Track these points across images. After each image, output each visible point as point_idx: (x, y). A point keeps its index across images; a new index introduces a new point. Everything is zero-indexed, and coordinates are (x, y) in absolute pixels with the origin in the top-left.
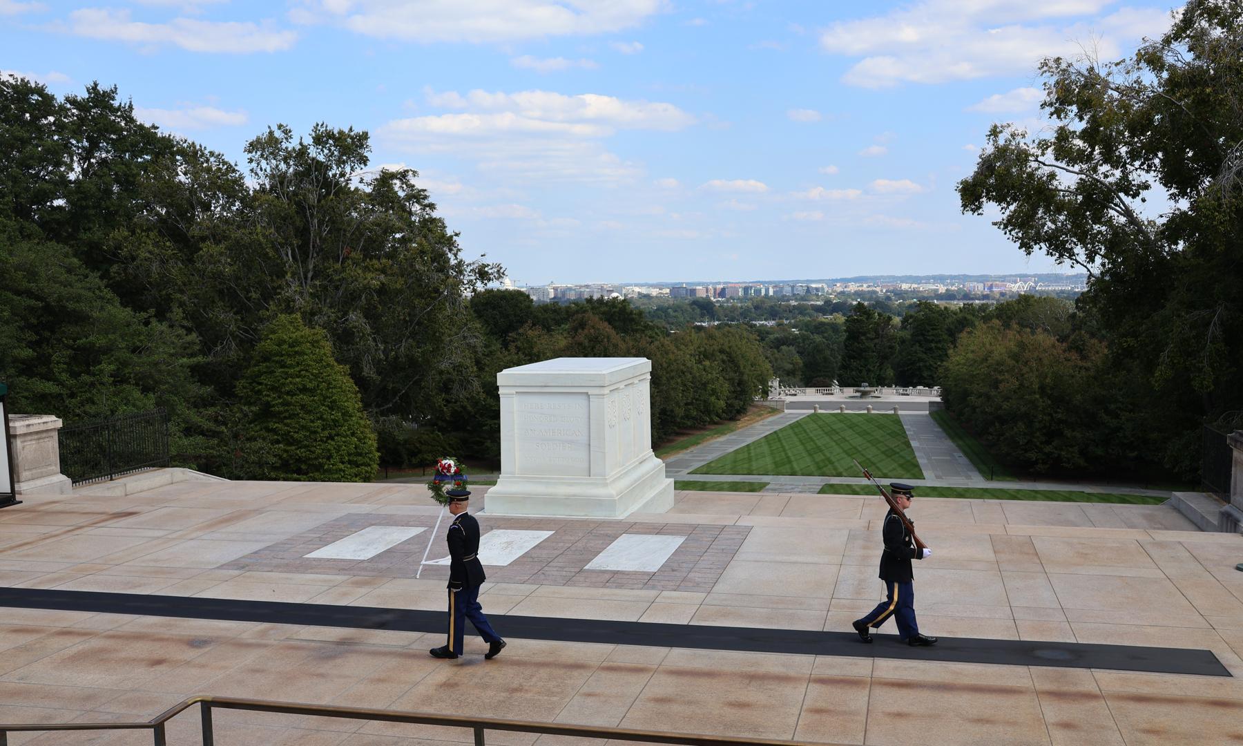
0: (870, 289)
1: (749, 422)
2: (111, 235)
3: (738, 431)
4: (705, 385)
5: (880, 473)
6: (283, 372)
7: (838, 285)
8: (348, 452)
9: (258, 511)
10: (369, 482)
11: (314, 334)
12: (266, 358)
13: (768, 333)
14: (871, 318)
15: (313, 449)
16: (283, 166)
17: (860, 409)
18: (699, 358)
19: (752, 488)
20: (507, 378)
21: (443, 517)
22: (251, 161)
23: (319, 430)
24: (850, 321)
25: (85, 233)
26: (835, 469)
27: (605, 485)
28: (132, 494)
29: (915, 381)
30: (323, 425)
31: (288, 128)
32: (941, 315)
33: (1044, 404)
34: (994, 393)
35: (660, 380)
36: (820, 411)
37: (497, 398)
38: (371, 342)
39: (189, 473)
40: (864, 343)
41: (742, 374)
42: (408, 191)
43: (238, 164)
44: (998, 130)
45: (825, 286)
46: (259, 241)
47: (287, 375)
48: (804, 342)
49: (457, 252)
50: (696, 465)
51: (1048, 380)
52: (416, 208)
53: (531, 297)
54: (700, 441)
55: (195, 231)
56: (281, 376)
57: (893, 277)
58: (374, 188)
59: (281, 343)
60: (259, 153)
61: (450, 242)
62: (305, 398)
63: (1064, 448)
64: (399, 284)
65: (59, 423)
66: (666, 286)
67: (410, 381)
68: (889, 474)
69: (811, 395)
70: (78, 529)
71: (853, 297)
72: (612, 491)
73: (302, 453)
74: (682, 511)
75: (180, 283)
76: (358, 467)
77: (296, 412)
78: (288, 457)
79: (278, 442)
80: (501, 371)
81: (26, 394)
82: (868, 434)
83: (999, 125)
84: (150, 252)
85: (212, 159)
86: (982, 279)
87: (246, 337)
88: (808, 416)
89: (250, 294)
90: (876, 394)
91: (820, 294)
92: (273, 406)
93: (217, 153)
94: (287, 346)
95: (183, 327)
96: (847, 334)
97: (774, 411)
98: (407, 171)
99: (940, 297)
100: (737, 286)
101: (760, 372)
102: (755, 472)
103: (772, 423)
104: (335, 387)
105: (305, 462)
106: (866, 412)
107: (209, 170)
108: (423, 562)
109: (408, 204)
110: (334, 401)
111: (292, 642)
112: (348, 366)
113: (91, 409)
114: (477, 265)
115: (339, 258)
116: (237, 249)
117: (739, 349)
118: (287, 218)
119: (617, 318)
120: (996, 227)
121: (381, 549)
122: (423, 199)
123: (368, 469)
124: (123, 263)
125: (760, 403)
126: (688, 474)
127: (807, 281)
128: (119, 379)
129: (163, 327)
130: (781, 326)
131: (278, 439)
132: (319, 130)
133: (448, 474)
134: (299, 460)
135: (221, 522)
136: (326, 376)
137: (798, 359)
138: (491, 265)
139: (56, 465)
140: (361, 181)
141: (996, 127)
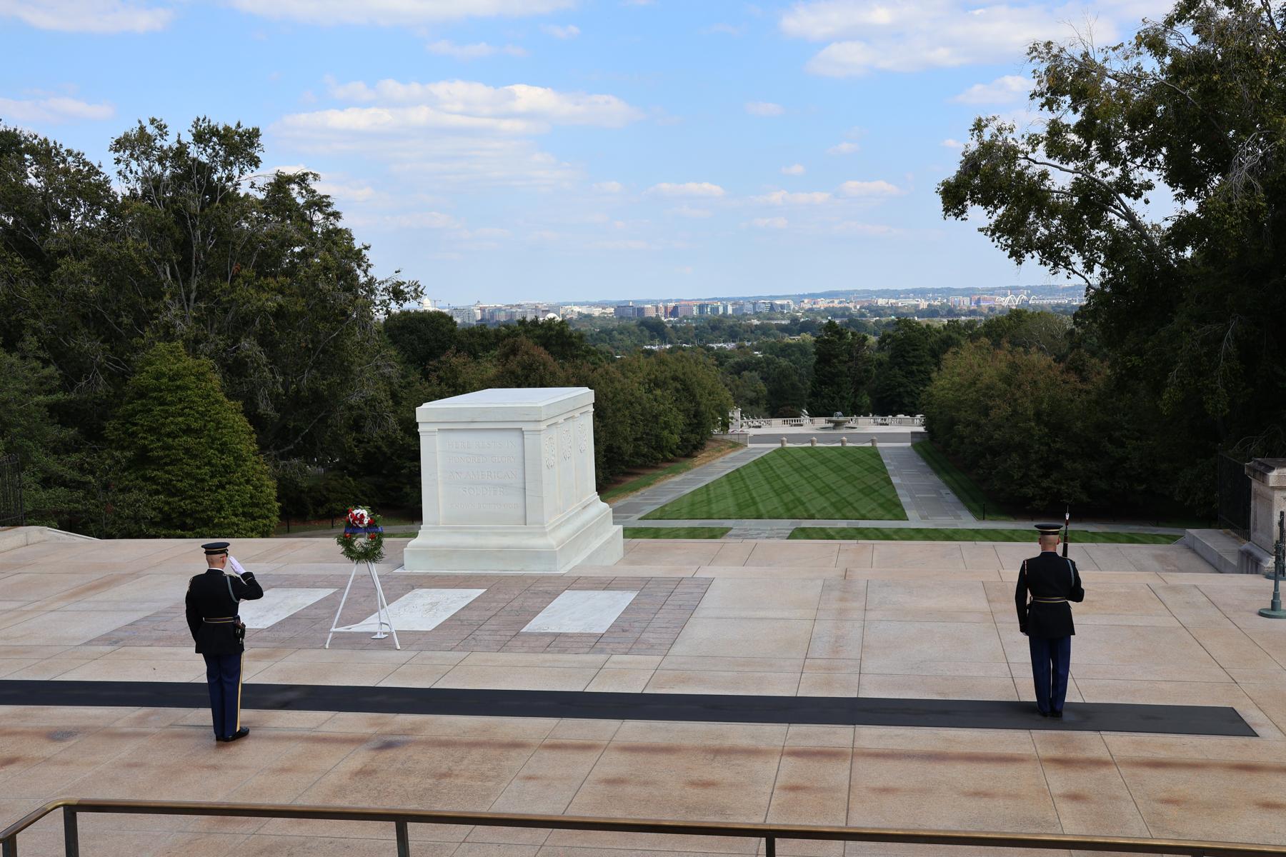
0: (842, 305)
1: (708, 459)
3: (695, 469)
4: (656, 417)
5: (857, 514)
6: (162, 410)
7: (806, 301)
8: (242, 503)
9: (135, 575)
12: (142, 394)
13: (727, 357)
14: (843, 339)
15: (199, 500)
16: (157, 168)
17: (833, 442)
18: (649, 387)
19: (713, 534)
20: (427, 413)
21: (355, 576)
22: (118, 161)
24: (820, 342)
26: (807, 510)
27: (544, 534)
29: (895, 409)
30: (212, 472)
31: (162, 123)
32: (923, 334)
33: (1040, 433)
34: (984, 421)
35: (604, 413)
36: (788, 445)
37: (417, 436)
40: (836, 367)
41: (698, 404)
42: (308, 197)
43: (102, 165)
44: (983, 124)
45: (791, 303)
46: (130, 256)
47: (168, 414)
48: (768, 367)
49: (367, 268)
50: (649, 509)
51: (1044, 406)
52: (318, 217)
53: (455, 319)
54: (652, 482)
55: (51, 245)
56: (160, 415)
57: (868, 291)
58: (268, 194)
59: (159, 375)
60: (128, 152)
61: (358, 256)
62: (189, 440)
63: (1064, 481)
66: (610, 304)
67: (314, 419)
68: (868, 515)
69: (777, 427)
71: (823, 314)
72: (552, 541)
73: (186, 504)
74: (633, 563)
75: (33, 306)
79: (157, 492)
80: (421, 405)
82: (843, 469)
83: (984, 118)
85: (70, 159)
86: (968, 292)
88: (774, 451)
89: (120, 319)
90: (852, 424)
91: (785, 311)
92: (151, 450)
93: (75, 152)
94: (167, 380)
95: (38, 358)
96: (817, 356)
97: (735, 445)
98: (307, 174)
99: (921, 313)
100: (690, 303)
101: (718, 402)
102: (715, 516)
103: (733, 459)
104: (225, 427)
105: (190, 515)
106: (840, 445)
107: (66, 172)
108: (333, 629)
109: (308, 213)
110: (224, 444)
111: (176, 730)
112: (240, 402)
114: (390, 283)
116: (104, 266)
117: (695, 375)
118: (164, 230)
119: (554, 342)
120: (983, 233)
121: (284, 615)
122: (325, 206)
125: (719, 437)
126: (639, 519)
127: (771, 297)
130: (742, 349)
132: (201, 126)
133: (361, 526)
134: (184, 513)
136: (214, 414)
137: (762, 386)
138: (407, 283)
140: (253, 186)
141: (980, 120)
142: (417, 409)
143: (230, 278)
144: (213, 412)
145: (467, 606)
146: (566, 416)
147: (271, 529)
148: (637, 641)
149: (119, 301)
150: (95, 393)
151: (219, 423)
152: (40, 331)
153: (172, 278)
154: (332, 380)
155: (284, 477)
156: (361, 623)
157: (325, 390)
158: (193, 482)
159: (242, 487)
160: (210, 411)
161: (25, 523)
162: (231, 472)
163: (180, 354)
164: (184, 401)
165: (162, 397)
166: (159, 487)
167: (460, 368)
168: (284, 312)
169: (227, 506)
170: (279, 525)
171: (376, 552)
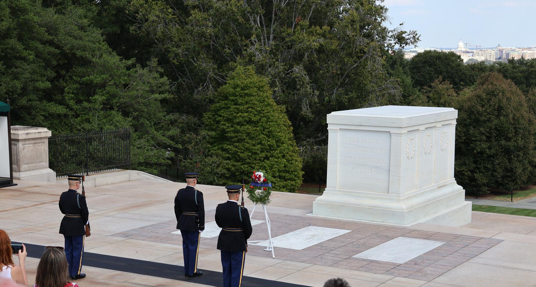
2: (132, 3)
6: (235, 108)
8: (279, 170)
11: (260, 81)
15: (253, 165)
21: (254, 212)
23: (258, 152)
28: (99, 186)
39: (143, 175)
47: (239, 111)
49: (381, 21)
53: (462, 57)
56: (234, 111)
59: (236, 86)
62: (249, 128)
64: (334, 45)
65: (49, 134)
70: (41, 204)
72: (403, 206)
73: (245, 168)
74: (474, 227)
76: (286, 180)
77: (243, 138)
78: (235, 170)
79: (228, 159)
81: (43, 113)
84: (158, 16)
87: (222, 81)
89: (224, 50)
92: (227, 132)
95: (157, 72)
104: (272, 121)
113: (87, 126)
114: (396, 32)
115: (292, 24)
116: (219, 16)
123: (293, 183)
124: (139, 23)
128: (109, 106)
129: (146, 70)
131: (228, 156)
133: (259, 182)
134: (243, 173)
135: (134, 207)
136: (266, 113)
139: (46, 162)
142: (328, 116)
143: (293, 26)
144: (266, 111)
145: (332, 239)
147: (296, 188)
148: (419, 271)
149: (224, 38)
150: (207, 95)
151: (269, 118)
152: (178, 55)
153: (261, 25)
154: (352, 95)
155: (316, 156)
156: (266, 241)
157: (346, 101)
158: (250, 154)
159: (279, 159)
160: (264, 111)
161: (131, 168)
162: (274, 150)
163: (250, 73)
164: (249, 103)
165: (236, 99)
166: (230, 156)
167: (443, 92)
168: (324, 50)
170: (302, 186)
171: (266, 198)
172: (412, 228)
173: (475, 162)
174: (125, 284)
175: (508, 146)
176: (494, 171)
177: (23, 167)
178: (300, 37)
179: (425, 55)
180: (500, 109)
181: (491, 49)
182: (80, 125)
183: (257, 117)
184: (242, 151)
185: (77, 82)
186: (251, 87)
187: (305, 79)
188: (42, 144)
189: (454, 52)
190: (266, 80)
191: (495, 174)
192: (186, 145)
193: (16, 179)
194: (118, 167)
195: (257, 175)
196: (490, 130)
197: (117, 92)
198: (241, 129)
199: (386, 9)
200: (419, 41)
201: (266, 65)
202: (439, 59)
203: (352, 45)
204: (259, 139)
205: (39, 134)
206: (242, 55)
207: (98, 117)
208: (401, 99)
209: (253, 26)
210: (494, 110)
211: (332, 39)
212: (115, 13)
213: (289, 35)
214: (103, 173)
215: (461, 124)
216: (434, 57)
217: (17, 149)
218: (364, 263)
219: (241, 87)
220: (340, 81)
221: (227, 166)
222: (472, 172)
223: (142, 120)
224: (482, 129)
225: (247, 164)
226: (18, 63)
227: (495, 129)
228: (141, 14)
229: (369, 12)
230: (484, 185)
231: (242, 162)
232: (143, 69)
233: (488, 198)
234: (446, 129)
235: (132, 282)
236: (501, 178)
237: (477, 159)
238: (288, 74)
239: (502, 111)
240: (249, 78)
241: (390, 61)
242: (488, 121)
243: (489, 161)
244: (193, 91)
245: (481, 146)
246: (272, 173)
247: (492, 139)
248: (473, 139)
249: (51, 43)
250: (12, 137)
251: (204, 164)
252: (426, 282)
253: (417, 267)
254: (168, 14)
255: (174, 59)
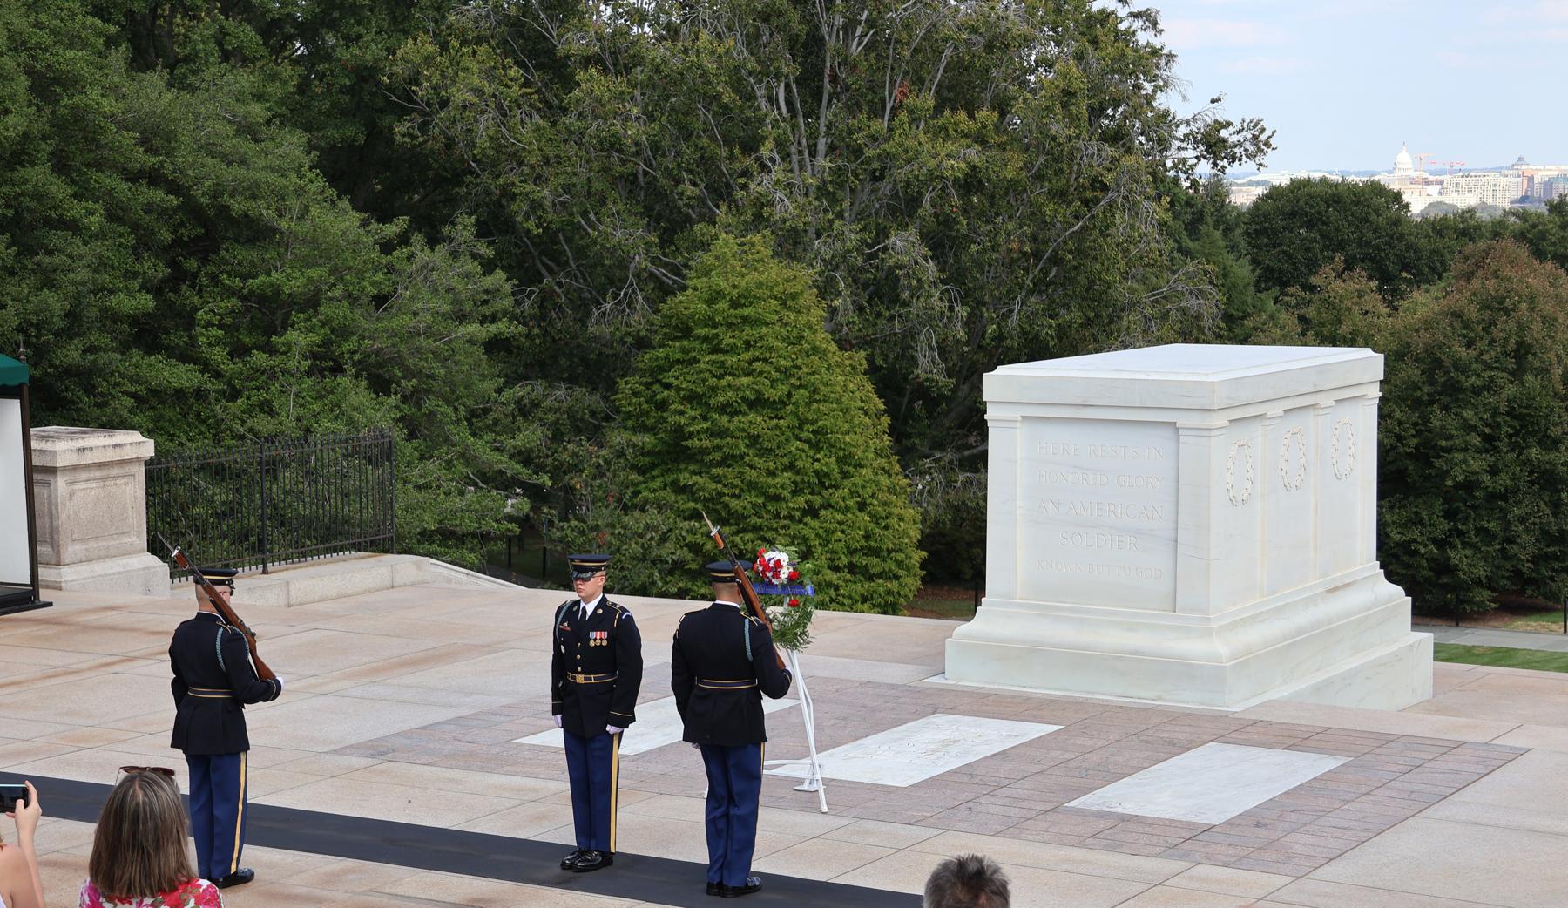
2: (399, 53)
6: (715, 362)
8: (848, 547)
9: (489, 648)
10: (894, 613)
15: (769, 535)
23: (786, 493)
25: (348, 47)
28: (301, 604)
38: (936, 302)
39: (433, 568)
46: (700, 67)
47: (724, 371)
49: (1154, 92)
53: (1406, 198)
56: (711, 372)
59: (714, 297)
62: (756, 421)
64: (1012, 167)
65: (148, 448)
72: (1219, 648)
73: (745, 540)
74: (1441, 710)
76: (870, 578)
77: (737, 452)
79: (696, 515)
84: (478, 91)
87: (675, 281)
89: (680, 188)
92: (691, 435)
95: (474, 256)
113: (264, 424)
114: (1200, 124)
116: (662, 84)
118: (769, 15)
123: (893, 585)
124: (425, 114)
128: (330, 363)
129: (441, 252)
142: (985, 375)
143: (888, 111)
144: (806, 370)
145: (1004, 752)
146: (1289, 404)
149: (678, 153)
150: (628, 324)
151: (815, 391)
154: (1068, 318)
155: (964, 503)
158: (760, 501)
159: (850, 515)
162: (834, 486)
163: (756, 257)
165: (717, 335)
166: (699, 506)
167: (1349, 303)
168: (980, 182)
169: (819, 549)
170: (920, 594)
171: (799, 631)
172: (1248, 717)
173: (1450, 515)
174: (371, 898)
175: (1549, 463)
176: (1510, 541)
177: (71, 550)
178: (909, 144)
179: (1292, 192)
180: (1522, 351)
181: (1498, 170)
182: (243, 422)
183: (780, 386)
184: (737, 492)
185: (232, 292)
186: (759, 298)
187: (925, 270)
188: (125, 480)
189: (1382, 183)
190: (805, 275)
191: (1513, 549)
192: (567, 477)
193: (48, 587)
194: (358, 547)
195: (769, 560)
196: (1493, 416)
197: (354, 320)
198: (732, 426)
199: (1170, 56)
200: (1269, 150)
201: (806, 231)
202: (1335, 202)
203: (1065, 166)
204: (785, 455)
205: (118, 449)
206: (732, 203)
207: (297, 395)
208: (1218, 327)
209: (766, 115)
210: (1506, 354)
211: (1004, 150)
212: (348, 83)
213: (874, 138)
214: (312, 565)
215: (1404, 400)
216: (1322, 200)
217: (50, 496)
218: (1102, 824)
219: (732, 299)
220: (1031, 276)
221: (690, 538)
222: (1441, 544)
223: (430, 403)
224: (1468, 414)
225: (751, 531)
226: (55, 238)
227: (1508, 414)
228: (426, 84)
229: (1117, 66)
230: (1479, 583)
231: (738, 525)
232: (433, 250)
233: (1492, 623)
234: (1346, 413)
235: (393, 891)
236: (1532, 562)
237: (1456, 504)
238: (874, 256)
239: (1530, 357)
240: (755, 269)
241: (1186, 213)
242: (1487, 388)
243: (1492, 509)
244: (588, 314)
245: (1468, 466)
246: (829, 555)
247: (1500, 444)
248: (1443, 443)
249: (154, 178)
250: (36, 461)
251: (619, 533)
252: (1289, 879)
253: (1262, 832)
254: (509, 83)
255: (527, 218)
